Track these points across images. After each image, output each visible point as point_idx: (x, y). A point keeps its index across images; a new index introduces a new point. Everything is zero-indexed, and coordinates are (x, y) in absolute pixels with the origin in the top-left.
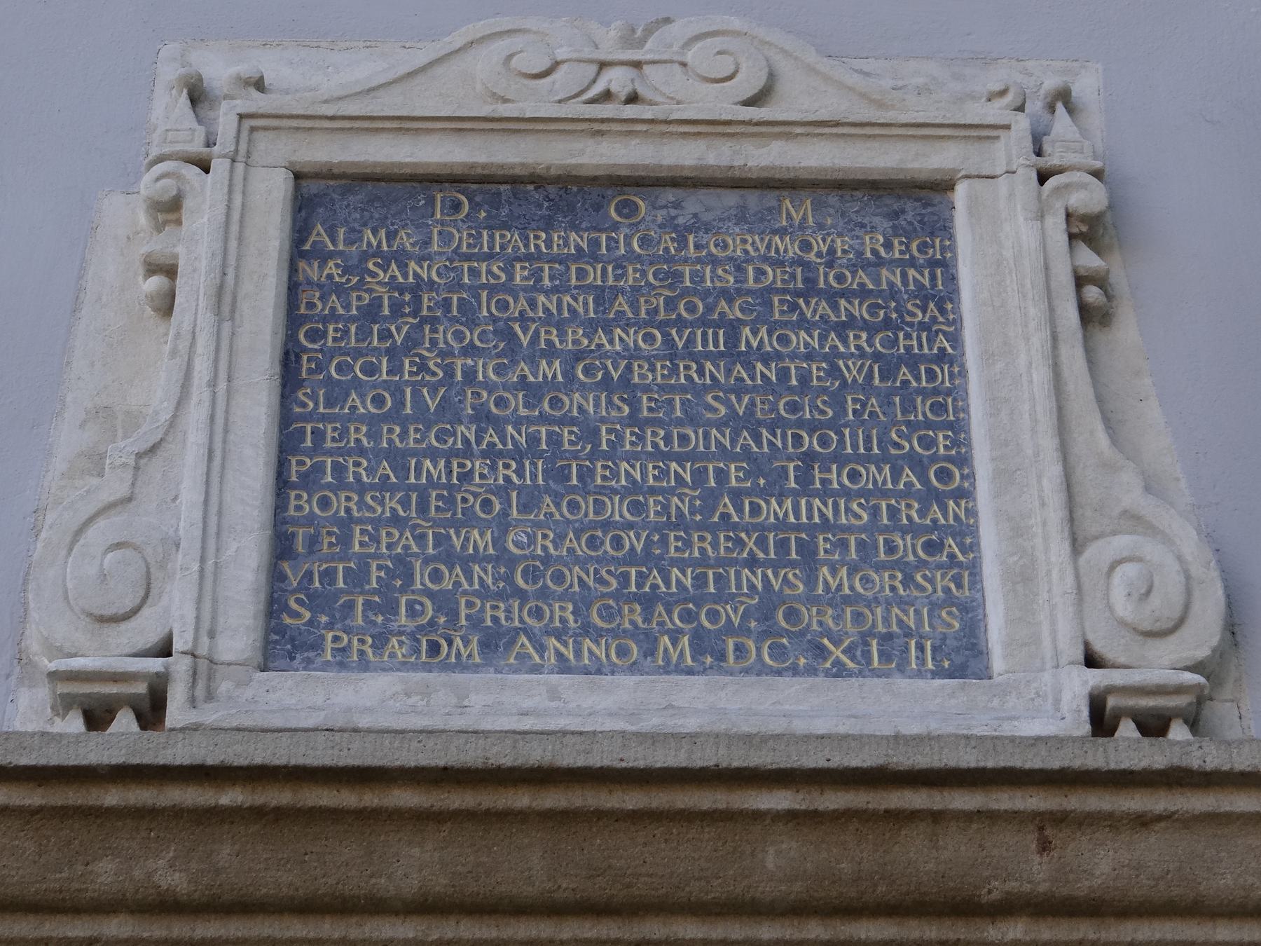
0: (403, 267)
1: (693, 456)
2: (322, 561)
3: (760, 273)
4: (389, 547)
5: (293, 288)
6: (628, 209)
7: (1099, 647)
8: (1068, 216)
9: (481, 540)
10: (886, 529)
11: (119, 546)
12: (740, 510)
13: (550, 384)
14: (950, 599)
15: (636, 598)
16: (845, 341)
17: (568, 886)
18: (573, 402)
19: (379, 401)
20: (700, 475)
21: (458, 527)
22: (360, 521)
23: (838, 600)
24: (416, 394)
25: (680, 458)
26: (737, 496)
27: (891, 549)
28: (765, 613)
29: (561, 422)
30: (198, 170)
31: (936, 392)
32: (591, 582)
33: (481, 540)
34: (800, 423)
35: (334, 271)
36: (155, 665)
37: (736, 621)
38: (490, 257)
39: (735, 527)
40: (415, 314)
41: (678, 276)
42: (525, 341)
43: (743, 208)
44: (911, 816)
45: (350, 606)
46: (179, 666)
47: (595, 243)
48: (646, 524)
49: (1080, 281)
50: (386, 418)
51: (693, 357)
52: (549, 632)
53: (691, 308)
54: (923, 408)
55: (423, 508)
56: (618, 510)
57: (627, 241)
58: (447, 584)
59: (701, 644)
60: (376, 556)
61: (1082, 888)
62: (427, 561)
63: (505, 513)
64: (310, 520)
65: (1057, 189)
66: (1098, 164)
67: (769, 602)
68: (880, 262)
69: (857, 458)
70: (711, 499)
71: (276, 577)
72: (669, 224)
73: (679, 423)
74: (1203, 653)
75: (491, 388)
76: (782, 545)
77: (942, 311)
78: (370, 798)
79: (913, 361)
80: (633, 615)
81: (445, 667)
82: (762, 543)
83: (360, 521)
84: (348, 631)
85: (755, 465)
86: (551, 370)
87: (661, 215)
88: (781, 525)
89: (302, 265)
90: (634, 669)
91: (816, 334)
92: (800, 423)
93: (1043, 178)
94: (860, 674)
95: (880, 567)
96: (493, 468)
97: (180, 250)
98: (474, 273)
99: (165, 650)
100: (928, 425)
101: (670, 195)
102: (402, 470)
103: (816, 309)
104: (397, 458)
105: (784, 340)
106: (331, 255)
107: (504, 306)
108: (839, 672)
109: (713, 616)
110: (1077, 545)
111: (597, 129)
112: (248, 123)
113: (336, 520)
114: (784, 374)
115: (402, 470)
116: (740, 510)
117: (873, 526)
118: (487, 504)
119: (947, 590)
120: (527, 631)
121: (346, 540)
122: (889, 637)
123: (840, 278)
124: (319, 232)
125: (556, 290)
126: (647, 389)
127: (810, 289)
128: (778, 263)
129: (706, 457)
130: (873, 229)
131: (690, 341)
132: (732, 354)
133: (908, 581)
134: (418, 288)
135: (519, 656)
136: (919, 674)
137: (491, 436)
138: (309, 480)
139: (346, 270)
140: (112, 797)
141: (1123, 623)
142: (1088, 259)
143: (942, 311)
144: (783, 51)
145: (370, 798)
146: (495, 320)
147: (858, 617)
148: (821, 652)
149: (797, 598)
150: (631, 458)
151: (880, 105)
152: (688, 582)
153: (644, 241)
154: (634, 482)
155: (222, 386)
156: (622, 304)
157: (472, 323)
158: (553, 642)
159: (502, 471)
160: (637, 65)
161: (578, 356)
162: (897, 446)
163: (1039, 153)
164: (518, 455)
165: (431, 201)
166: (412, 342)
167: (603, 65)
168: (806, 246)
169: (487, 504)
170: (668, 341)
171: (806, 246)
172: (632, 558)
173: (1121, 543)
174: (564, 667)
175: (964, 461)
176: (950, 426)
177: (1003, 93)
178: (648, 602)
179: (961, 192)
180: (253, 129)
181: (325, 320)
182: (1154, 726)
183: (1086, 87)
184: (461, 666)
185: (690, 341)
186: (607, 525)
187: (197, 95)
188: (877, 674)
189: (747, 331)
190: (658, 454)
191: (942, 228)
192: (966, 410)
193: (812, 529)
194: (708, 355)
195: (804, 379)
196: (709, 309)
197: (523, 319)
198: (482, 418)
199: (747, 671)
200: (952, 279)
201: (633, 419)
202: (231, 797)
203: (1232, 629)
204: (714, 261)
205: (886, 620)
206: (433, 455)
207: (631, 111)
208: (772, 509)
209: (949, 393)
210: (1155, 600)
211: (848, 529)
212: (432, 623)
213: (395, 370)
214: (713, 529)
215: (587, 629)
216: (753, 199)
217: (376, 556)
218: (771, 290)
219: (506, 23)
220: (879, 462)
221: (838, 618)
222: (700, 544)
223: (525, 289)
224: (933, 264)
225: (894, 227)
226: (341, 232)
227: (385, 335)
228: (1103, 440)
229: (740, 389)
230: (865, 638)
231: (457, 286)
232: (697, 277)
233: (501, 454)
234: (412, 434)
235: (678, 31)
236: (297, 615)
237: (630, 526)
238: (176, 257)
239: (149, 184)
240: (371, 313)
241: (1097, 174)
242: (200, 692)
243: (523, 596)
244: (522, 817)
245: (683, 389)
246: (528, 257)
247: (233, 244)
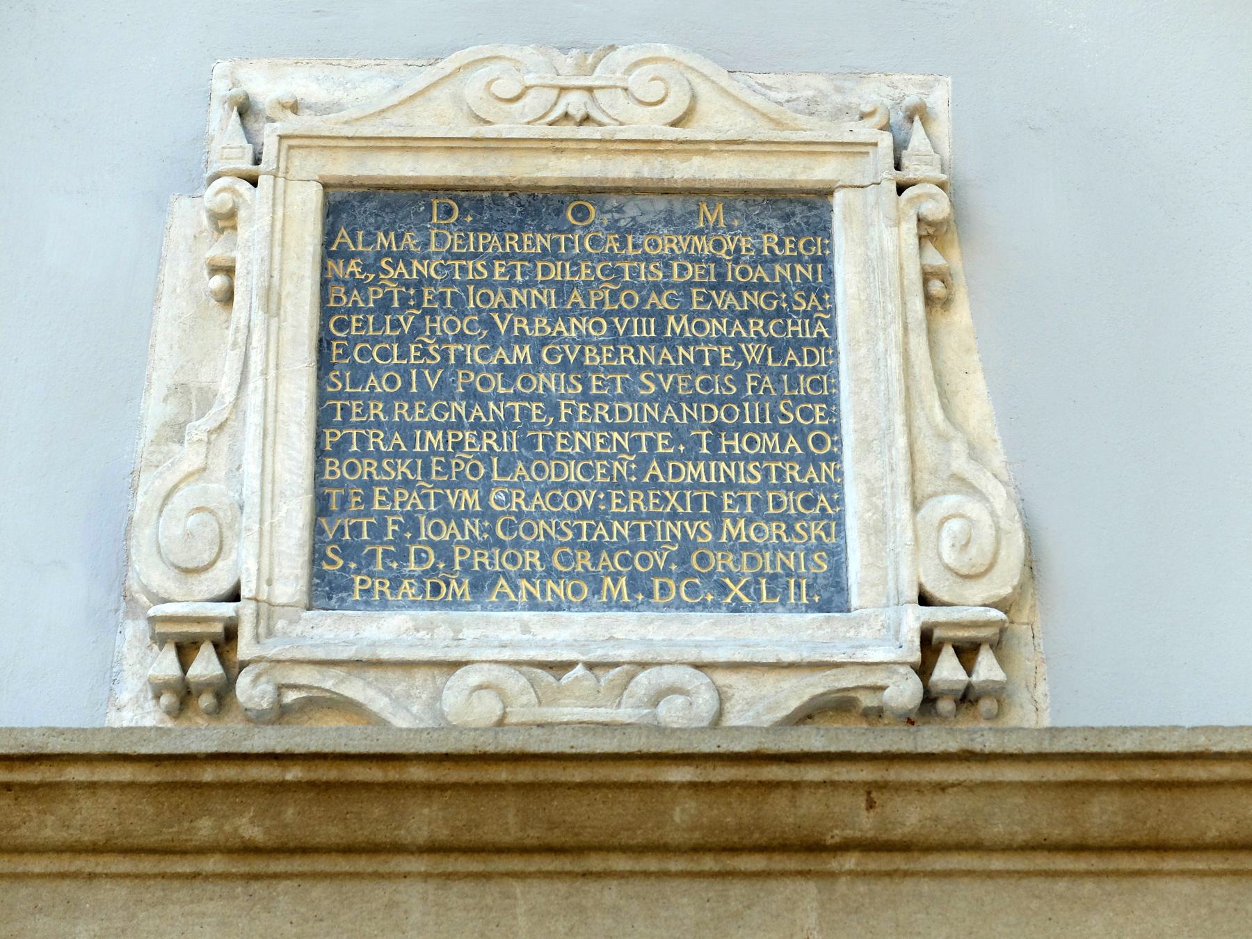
0: (408, 265)
1: (630, 427)
2: (351, 517)
3: (683, 269)
4: (402, 505)
5: (324, 284)
6: (581, 213)
7: (930, 588)
8: (919, 220)
9: (471, 499)
10: (774, 488)
11: (199, 509)
12: (665, 472)
13: (521, 366)
14: (821, 546)
15: (587, 546)
16: (746, 327)
17: (534, 835)
18: (540, 381)
19: (391, 381)
20: (635, 442)
21: (451, 486)
22: (379, 483)
23: (737, 547)
24: (420, 375)
25: (620, 429)
26: (663, 459)
27: (778, 504)
28: (682, 558)
29: (532, 398)
30: (248, 185)
31: (815, 371)
32: (553, 533)
33: (471, 499)
34: (711, 399)
35: (356, 270)
36: (228, 609)
37: (661, 564)
38: (475, 256)
39: (661, 486)
40: (418, 306)
41: (619, 271)
42: (503, 329)
43: (670, 212)
44: (776, 785)
45: (373, 554)
46: (245, 610)
47: (556, 243)
48: (594, 485)
49: (927, 276)
50: (397, 396)
51: (631, 342)
52: (522, 575)
53: (630, 300)
54: (805, 382)
55: (426, 473)
56: (573, 472)
57: (581, 242)
58: (445, 536)
59: (636, 582)
60: (392, 513)
61: (897, 834)
62: (430, 516)
63: (488, 476)
64: (341, 483)
65: (911, 200)
66: (944, 177)
67: (687, 546)
68: (775, 259)
69: (753, 428)
70: (643, 462)
71: (317, 530)
72: (613, 227)
73: (620, 399)
74: (1006, 591)
75: (476, 369)
76: (697, 501)
77: (821, 301)
78: (392, 774)
79: (797, 344)
80: (583, 560)
81: (445, 605)
82: (681, 499)
83: (379, 483)
84: (371, 575)
85: (678, 435)
86: (523, 353)
87: (606, 219)
88: (696, 485)
89: (330, 263)
90: (585, 606)
91: (725, 321)
92: (711, 399)
93: (901, 189)
94: (753, 609)
95: (769, 519)
96: (479, 438)
97: (237, 255)
98: (463, 270)
99: (234, 596)
100: (808, 399)
101: (614, 201)
102: (410, 441)
103: (726, 300)
104: (406, 430)
105: (700, 327)
106: (353, 255)
107: (485, 298)
108: (737, 607)
109: (644, 560)
110: (916, 507)
111: (556, 147)
112: (286, 143)
113: (360, 483)
114: (700, 356)
115: (410, 441)
116: (665, 472)
117: (765, 486)
118: (474, 469)
119: (818, 538)
120: (505, 574)
121: (368, 499)
122: (773, 578)
123: (744, 273)
124: (343, 236)
125: (526, 285)
126: (595, 370)
127: (720, 284)
128: (696, 260)
129: (640, 427)
130: (770, 230)
131: (629, 329)
132: (660, 340)
133: (790, 530)
134: (419, 284)
135: (502, 596)
136: (796, 609)
137: (477, 412)
138: (340, 449)
139: (365, 269)
140: (208, 774)
141: (948, 568)
142: (934, 258)
143: (821, 301)
144: (702, 75)
145: (392, 774)
146: (479, 311)
147: (752, 560)
148: (724, 590)
149: (706, 545)
150: (583, 428)
151: (778, 124)
152: (626, 533)
153: (595, 242)
154: (585, 449)
155: (272, 372)
156: (576, 296)
157: (462, 314)
158: (524, 583)
159: (486, 441)
160: (590, 89)
161: (544, 341)
162: (784, 417)
163: (898, 167)
164: (498, 426)
165: (429, 207)
166: (416, 330)
167: (563, 89)
168: (718, 245)
169: (474, 469)
170: (612, 329)
171: (718, 245)
172: (584, 514)
173: (951, 501)
174: (533, 605)
175: (834, 429)
176: (824, 399)
177: (872, 114)
178: (595, 549)
179: (838, 199)
180: (290, 147)
181: (349, 312)
182: (967, 653)
183: (939, 99)
184: (456, 604)
185: (629, 329)
186: (565, 486)
187: (245, 110)
188: (767, 609)
189: (671, 319)
190: (604, 426)
191: (823, 229)
192: (837, 386)
193: (719, 488)
194: (642, 341)
195: (715, 360)
196: (644, 301)
197: (501, 310)
198: (471, 395)
199: (668, 606)
200: (829, 273)
201: (585, 396)
202: (293, 774)
203: (1031, 566)
204: (647, 259)
205: (773, 563)
206: (433, 427)
207: (585, 132)
208: (690, 471)
209: (824, 371)
210: (973, 550)
211: (746, 487)
212: (434, 568)
213: (403, 355)
214: (644, 488)
215: (550, 573)
216: (678, 205)
217: (392, 513)
218: (690, 283)
219: (487, 50)
220: (770, 430)
221: (737, 562)
222: (636, 500)
223: (503, 284)
224: (815, 260)
225: (786, 228)
226: (360, 234)
227: (396, 325)
228: (939, 415)
229: (666, 370)
230: (756, 577)
231: (450, 282)
232: (634, 273)
233: (485, 426)
234: (418, 411)
235: (621, 57)
236: (333, 563)
237: (582, 486)
238: (234, 260)
239: (215, 197)
240: (384, 306)
241: (942, 186)
242: (262, 630)
243: (502, 545)
244: (501, 787)
245: (622, 370)
246: (505, 256)
247: (277, 250)
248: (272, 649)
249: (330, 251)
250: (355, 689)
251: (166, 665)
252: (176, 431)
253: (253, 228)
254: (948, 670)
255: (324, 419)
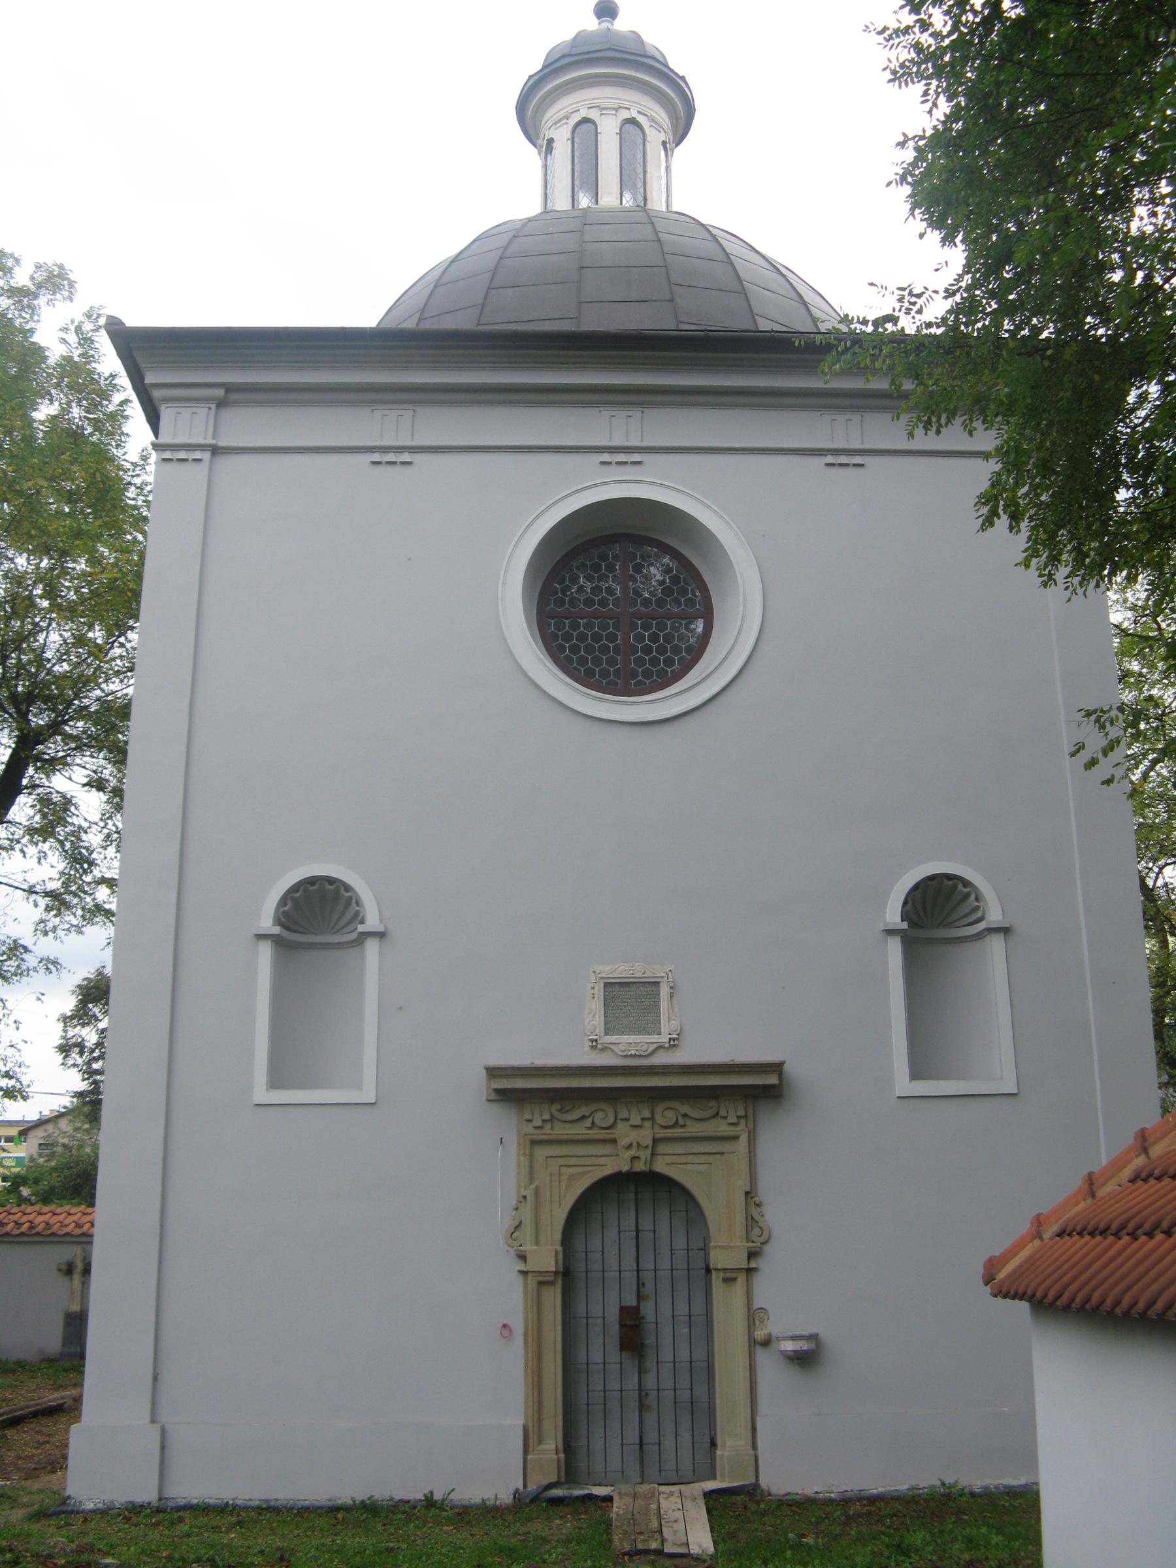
18: (629, 1007)
57: (632, 989)
110: (669, 1022)
173: (673, 1022)
182: (674, 1041)
187: (594, 972)
239: (592, 985)
248: (601, 1042)
249: (605, 991)
250: (610, 1046)
251: (590, 1044)
252: (589, 1013)
253: (596, 988)
254: (672, 1043)
255: (605, 1012)
